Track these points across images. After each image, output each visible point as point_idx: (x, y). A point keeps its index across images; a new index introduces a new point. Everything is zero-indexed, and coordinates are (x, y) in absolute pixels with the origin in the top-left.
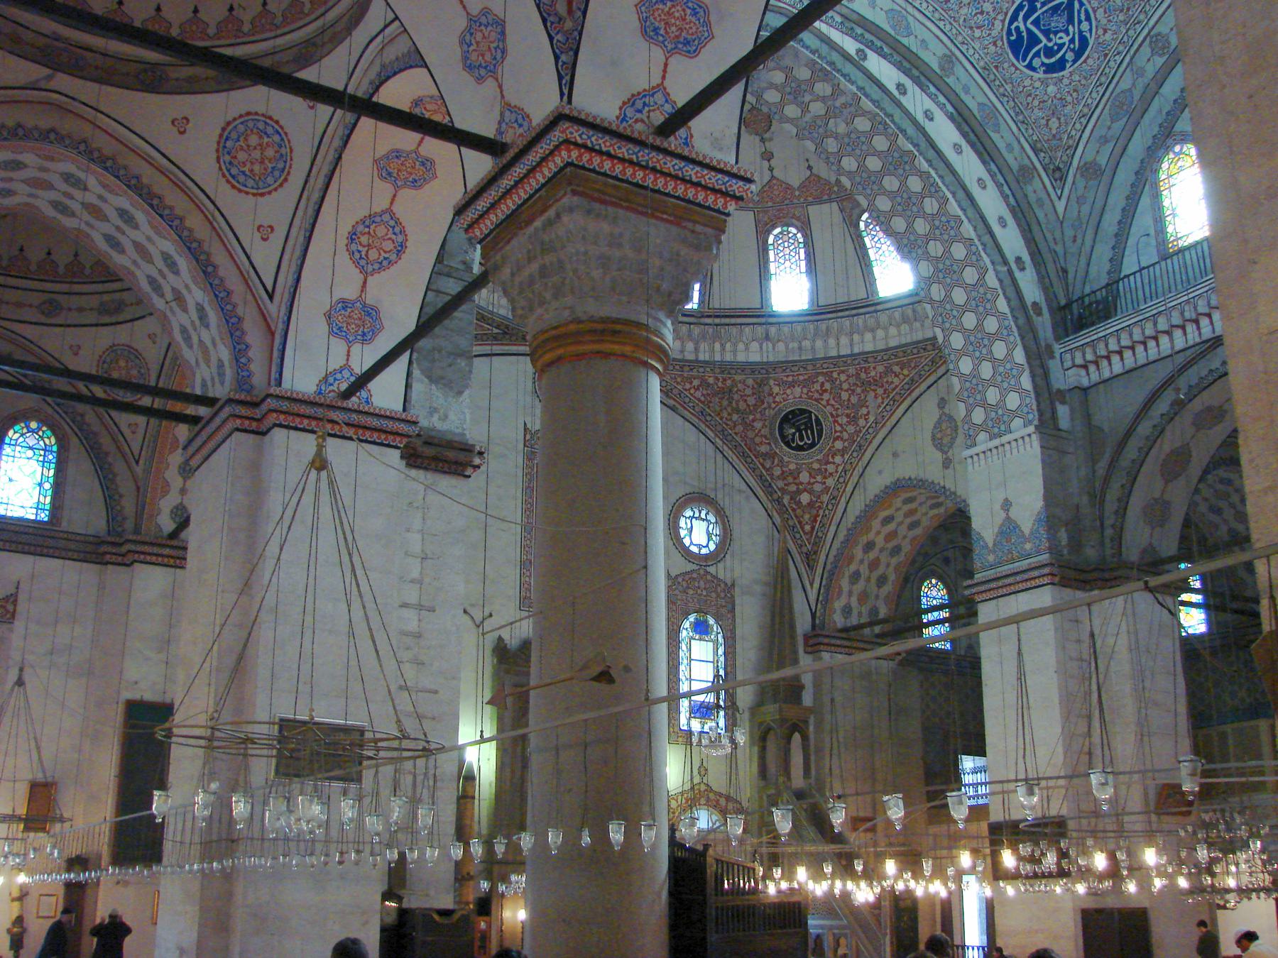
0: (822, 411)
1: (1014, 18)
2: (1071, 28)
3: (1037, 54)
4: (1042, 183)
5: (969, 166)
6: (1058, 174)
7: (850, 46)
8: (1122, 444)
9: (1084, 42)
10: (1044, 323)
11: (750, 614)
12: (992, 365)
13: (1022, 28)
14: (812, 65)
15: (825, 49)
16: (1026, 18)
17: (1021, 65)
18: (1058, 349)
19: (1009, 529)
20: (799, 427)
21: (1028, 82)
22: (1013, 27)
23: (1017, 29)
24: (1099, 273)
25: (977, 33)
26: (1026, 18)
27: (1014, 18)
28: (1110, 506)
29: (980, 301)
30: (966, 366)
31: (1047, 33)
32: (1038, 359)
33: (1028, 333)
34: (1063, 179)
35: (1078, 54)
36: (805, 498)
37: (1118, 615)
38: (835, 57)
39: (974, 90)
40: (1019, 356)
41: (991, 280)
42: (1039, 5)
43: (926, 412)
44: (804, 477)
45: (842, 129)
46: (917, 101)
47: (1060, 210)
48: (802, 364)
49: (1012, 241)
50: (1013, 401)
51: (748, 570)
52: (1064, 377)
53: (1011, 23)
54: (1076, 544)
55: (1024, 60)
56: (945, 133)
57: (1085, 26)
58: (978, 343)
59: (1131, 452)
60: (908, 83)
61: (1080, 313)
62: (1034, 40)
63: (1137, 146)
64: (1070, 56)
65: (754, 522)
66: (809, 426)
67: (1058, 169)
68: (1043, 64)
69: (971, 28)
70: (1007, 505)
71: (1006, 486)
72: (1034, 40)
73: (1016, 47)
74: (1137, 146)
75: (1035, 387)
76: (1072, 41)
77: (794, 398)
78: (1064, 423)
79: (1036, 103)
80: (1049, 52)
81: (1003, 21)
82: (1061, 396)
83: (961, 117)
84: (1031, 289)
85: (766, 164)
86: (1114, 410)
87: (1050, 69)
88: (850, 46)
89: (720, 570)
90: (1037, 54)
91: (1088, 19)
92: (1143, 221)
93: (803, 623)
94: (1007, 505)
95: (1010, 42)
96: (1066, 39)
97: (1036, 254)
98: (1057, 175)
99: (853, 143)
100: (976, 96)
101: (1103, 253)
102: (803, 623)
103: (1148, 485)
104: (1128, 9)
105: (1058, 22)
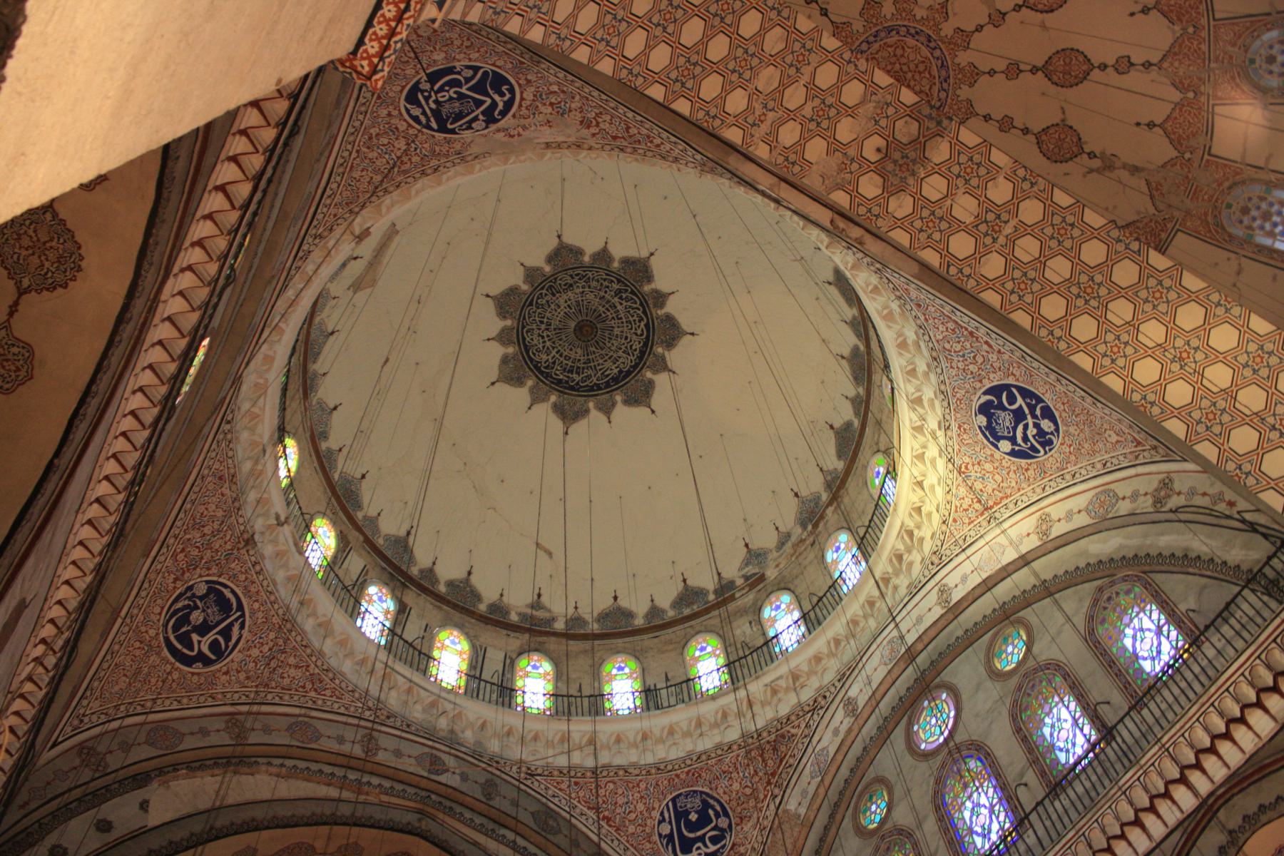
2: (433, 106)
13: (497, 97)
16: (494, 104)
17: (488, 68)
22: (508, 96)
23: (502, 95)
25: (555, 88)
31: (461, 96)
42: (481, 117)
53: (512, 100)
55: (486, 73)
57: (416, 112)
68: (459, 73)
69: (563, 92)
79: (457, 43)
81: (522, 99)
91: (416, 119)
95: (509, 83)
104: (370, 138)
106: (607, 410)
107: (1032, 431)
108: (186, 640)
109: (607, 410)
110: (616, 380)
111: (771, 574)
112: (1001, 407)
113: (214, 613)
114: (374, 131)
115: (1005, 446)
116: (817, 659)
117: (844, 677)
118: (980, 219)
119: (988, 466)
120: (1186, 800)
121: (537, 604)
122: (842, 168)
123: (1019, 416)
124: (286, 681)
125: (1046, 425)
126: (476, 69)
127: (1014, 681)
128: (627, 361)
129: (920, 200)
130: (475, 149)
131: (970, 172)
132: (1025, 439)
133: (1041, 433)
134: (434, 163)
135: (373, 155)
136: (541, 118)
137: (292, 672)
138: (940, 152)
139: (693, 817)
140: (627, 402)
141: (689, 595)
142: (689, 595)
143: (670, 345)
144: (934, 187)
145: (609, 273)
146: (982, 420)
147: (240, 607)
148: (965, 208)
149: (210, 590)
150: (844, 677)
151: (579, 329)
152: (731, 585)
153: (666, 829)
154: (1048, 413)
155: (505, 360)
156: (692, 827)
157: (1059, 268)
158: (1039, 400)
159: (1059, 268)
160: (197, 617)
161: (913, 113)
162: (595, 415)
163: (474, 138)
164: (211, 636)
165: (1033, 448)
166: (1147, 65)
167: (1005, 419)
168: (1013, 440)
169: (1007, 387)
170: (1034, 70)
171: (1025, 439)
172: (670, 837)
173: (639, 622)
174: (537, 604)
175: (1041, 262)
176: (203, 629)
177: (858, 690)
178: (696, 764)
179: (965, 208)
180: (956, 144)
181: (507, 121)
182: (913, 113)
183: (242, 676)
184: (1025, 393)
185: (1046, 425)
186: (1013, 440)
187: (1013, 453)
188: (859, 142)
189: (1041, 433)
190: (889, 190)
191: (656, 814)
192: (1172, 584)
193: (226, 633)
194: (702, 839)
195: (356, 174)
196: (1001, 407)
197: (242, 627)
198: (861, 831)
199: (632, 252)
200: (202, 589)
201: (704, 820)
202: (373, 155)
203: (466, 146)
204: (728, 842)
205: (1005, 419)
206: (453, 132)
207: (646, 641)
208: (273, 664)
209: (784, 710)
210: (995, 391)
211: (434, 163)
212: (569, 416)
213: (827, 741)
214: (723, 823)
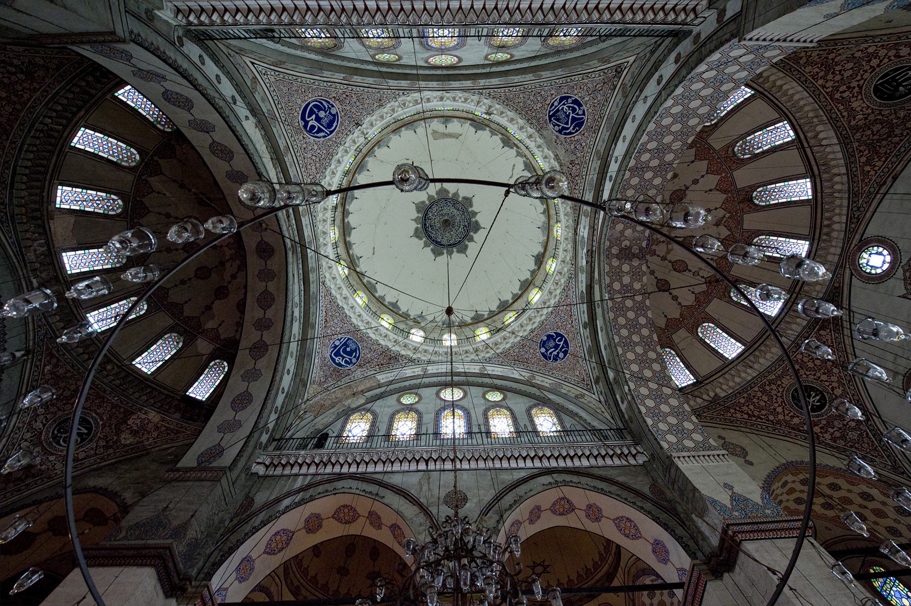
1: (570, 133)
3: (577, 114)
4: (626, 77)
5: (629, 129)
6: (618, 70)
9: (562, 99)
10: (686, 46)
15: (606, 224)
16: (568, 129)
21: (590, 110)
25: (584, 144)
26: (568, 129)
27: (570, 133)
31: (568, 116)
34: (619, 66)
35: (567, 98)
39: (603, 136)
46: (613, 167)
47: (632, 59)
49: (652, 89)
56: (620, 149)
57: (556, 104)
60: (608, 178)
62: (574, 119)
64: (570, 101)
67: (616, 71)
72: (574, 119)
73: (580, 125)
75: (717, 48)
76: (564, 104)
80: (574, 110)
83: (614, 138)
85: (701, 181)
87: (580, 105)
90: (577, 114)
91: (553, 104)
96: (565, 107)
98: (619, 70)
100: (604, 134)
105: (562, 116)
106: (426, 245)
107: (555, 353)
109: (426, 245)
110: (437, 242)
111: (423, 324)
112: (555, 340)
114: (543, 93)
115: (543, 350)
116: (426, 351)
117: (429, 362)
118: (626, 286)
119: (532, 351)
120: (553, 463)
121: (359, 258)
122: (617, 239)
123: (556, 347)
125: (561, 355)
126: (584, 114)
127: (491, 404)
128: (444, 242)
129: (620, 267)
130: (545, 133)
131: (636, 274)
132: (551, 353)
133: (557, 355)
134: (534, 121)
135: (532, 98)
136: (568, 147)
138: (635, 263)
139: (348, 349)
140: (432, 250)
141: (395, 305)
142: (395, 305)
143: (458, 252)
144: (626, 268)
145: (470, 219)
146: (545, 338)
148: (626, 280)
150: (429, 362)
151: (446, 221)
152: (409, 316)
153: (337, 343)
154: (565, 353)
155: (423, 202)
156: (345, 351)
157: (631, 315)
158: (568, 347)
159: (631, 315)
161: (641, 249)
162: (422, 242)
163: (551, 130)
165: (550, 358)
166: (680, 304)
167: (552, 344)
168: (547, 350)
169: (563, 336)
170: (656, 278)
171: (551, 353)
172: (336, 347)
173: (377, 295)
174: (359, 258)
175: (629, 309)
177: (432, 369)
178: (364, 338)
179: (626, 280)
180: (640, 265)
181: (562, 137)
182: (641, 249)
184: (566, 342)
185: (561, 355)
186: (547, 350)
187: (543, 354)
188: (626, 238)
189: (557, 355)
190: (617, 257)
191: (340, 336)
192: (566, 418)
194: (343, 357)
195: (521, 96)
196: (555, 340)
198: (399, 401)
199: (480, 222)
201: (350, 354)
202: (532, 98)
203: (546, 129)
204: (349, 367)
205: (552, 344)
206: (550, 120)
207: (374, 300)
209: (403, 353)
210: (558, 335)
211: (534, 121)
212: (417, 234)
213: (409, 372)
214: (354, 360)
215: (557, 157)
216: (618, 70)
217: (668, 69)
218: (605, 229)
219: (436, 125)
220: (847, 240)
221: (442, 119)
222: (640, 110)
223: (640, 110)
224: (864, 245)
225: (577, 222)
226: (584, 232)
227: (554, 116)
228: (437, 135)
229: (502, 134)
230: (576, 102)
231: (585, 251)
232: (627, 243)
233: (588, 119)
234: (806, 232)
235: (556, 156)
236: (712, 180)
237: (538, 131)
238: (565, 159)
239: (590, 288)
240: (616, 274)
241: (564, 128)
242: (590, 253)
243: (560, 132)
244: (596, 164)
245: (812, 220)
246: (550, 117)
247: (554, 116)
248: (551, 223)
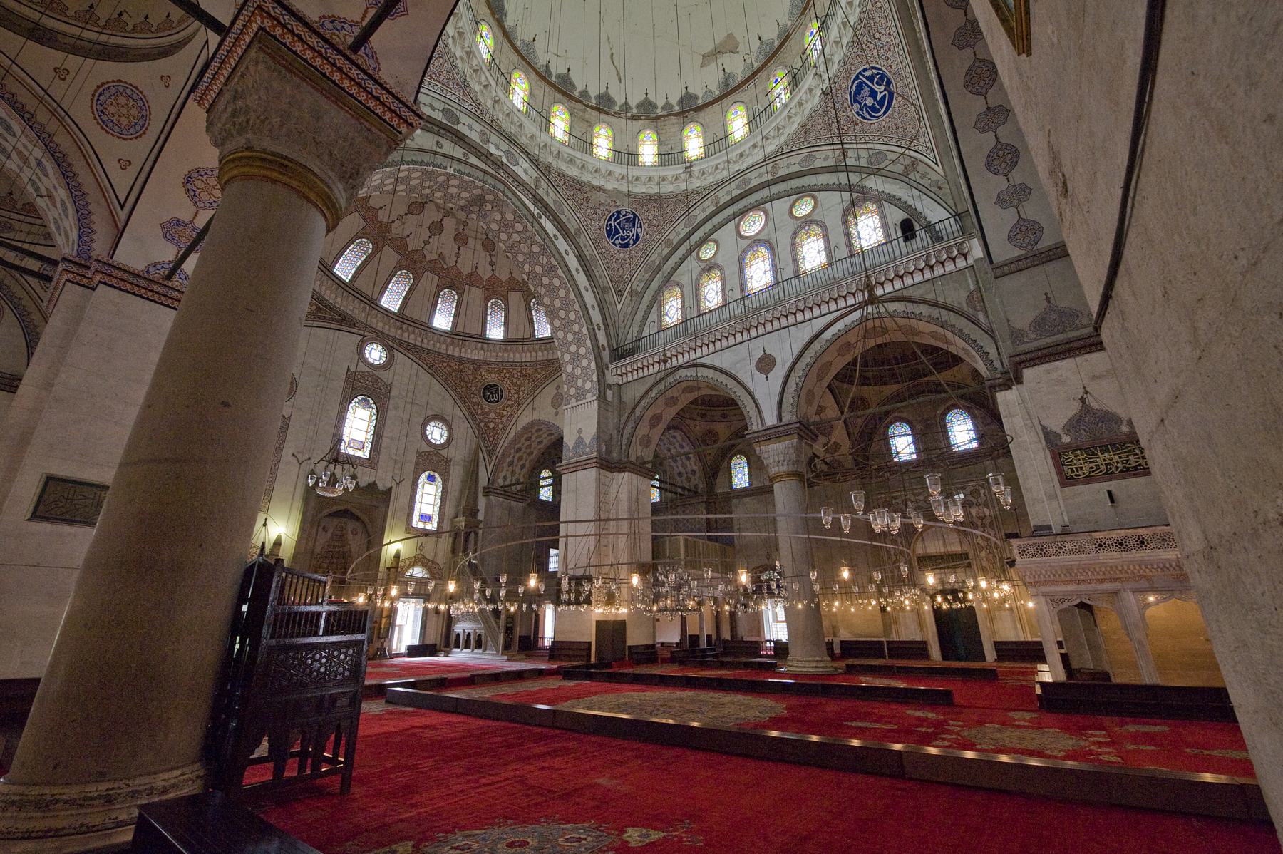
0: (505, 386)
5: (582, 280)
6: (620, 293)
7: (536, 211)
8: (633, 410)
10: (606, 355)
11: (457, 473)
12: (580, 368)
14: (514, 213)
15: (521, 207)
18: (610, 366)
19: (580, 441)
20: (492, 392)
24: (630, 338)
28: (626, 435)
29: (578, 341)
30: (569, 369)
32: (601, 368)
33: (598, 358)
34: (622, 295)
36: (491, 425)
37: (623, 482)
38: (526, 212)
40: (593, 365)
41: (585, 331)
43: (550, 391)
44: (492, 415)
45: (526, 249)
46: (562, 245)
47: (619, 307)
48: (497, 363)
49: (595, 315)
50: (588, 385)
51: (458, 455)
52: (612, 379)
54: (609, 451)
56: (573, 262)
58: (576, 358)
59: (638, 413)
61: (620, 353)
63: (655, 285)
65: (465, 432)
66: (497, 392)
70: (580, 431)
71: (580, 424)
73: (609, 233)
74: (655, 285)
77: (492, 378)
78: (609, 399)
80: (623, 239)
82: (609, 386)
83: (581, 258)
84: (603, 341)
86: (630, 395)
88: (536, 211)
89: (444, 452)
92: (653, 316)
93: (483, 481)
94: (580, 431)
97: (606, 325)
99: (530, 257)
100: (590, 251)
101: (636, 328)
102: (483, 481)
103: (643, 430)
108: (881, 103)
113: (866, 92)
124: (883, 21)
137: (877, 20)
147: (857, 77)
149: (856, 101)
160: (870, 101)
163: (626, 207)
164: (876, 87)
176: (873, 94)
181: (614, 210)
183: (890, 54)
188: (492, 211)
193: (871, 79)
197: (865, 70)
200: (856, 106)
208: (877, 35)
215: (600, 189)
216: (620, 293)
217: (603, 341)
218: (518, 203)
219: (737, 66)
220: (395, 340)
221: (733, 85)
222: (589, 298)
223: (589, 298)
224: (388, 349)
225: (534, 161)
226: (523, 169)
227: (632, 220)
228: (729, 46)
229: (658, 117)
230: (627, 245)
231: (504, 160)
232: (489, 207)
233: (607, 242)
234: (407, 313)
235: (604, 191)
236: (485, 272)
237: (635, 195)
238: (594, 196)
239: (460, 138)
240: (463, 186)
241: (618, 217)
242: (499, 165)
243: (618, 213)
244: (572, 226)
245: (412, 318)
246: (635, 216)
247: (632, 220)
248: (533, 75)
